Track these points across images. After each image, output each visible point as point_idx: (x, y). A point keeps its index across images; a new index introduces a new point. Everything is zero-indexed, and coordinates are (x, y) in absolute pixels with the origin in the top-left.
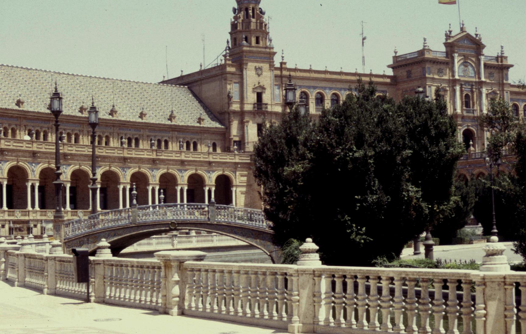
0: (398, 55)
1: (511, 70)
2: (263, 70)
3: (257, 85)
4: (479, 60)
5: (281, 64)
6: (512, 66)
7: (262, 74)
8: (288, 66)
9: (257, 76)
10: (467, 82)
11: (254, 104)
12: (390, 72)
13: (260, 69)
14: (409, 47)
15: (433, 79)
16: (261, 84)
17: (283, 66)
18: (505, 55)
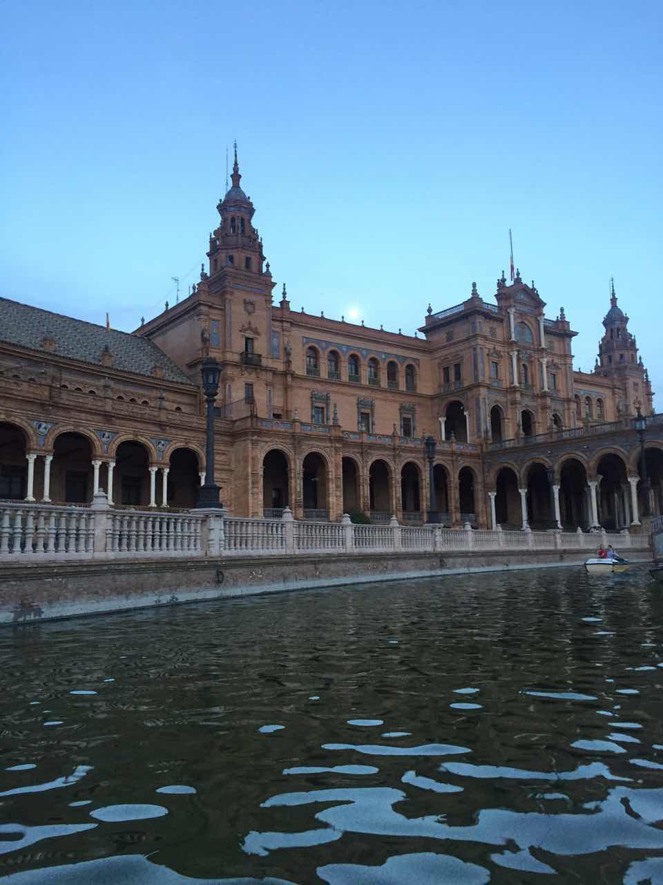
0: (432, 314)
1: (574, 338)
2: (256, 307)
3: (246, 326)
4: (538, 322)
5: (281, 303)
6: (575, 334)
8: (294, 307)
9: (247, 314)
10: (524, 348)
11: (242, 354)
12: (422, 336)
13: (252, 304)
14: (450, 298)
15: (485, 338)
16: (253, 326)
17: (285, 306)
18: (567, 320)
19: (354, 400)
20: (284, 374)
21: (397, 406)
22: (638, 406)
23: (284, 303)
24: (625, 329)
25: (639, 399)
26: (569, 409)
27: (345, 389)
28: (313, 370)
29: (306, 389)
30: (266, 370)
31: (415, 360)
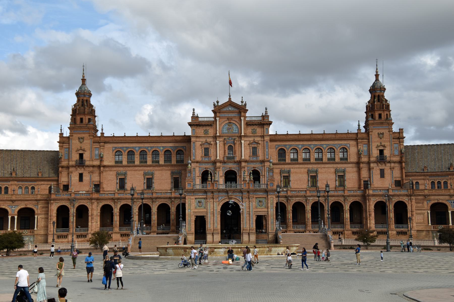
3: (80, 148)
7: (83, 142)
8: (105, 135)
13: (83, 138)
16: (83, 148)
18: (268, 114)
19: (142, 172)
20: (99, 167)
21: (169, 172)
22: (381, 148)
23: (102, 134)
24: (383, 96)
25: (383, 144)
26: (264, 166)
27: (136, 168)
28: (118, 163)
29: (114, 171)
30: (88, 166)
31: (183, 147)
